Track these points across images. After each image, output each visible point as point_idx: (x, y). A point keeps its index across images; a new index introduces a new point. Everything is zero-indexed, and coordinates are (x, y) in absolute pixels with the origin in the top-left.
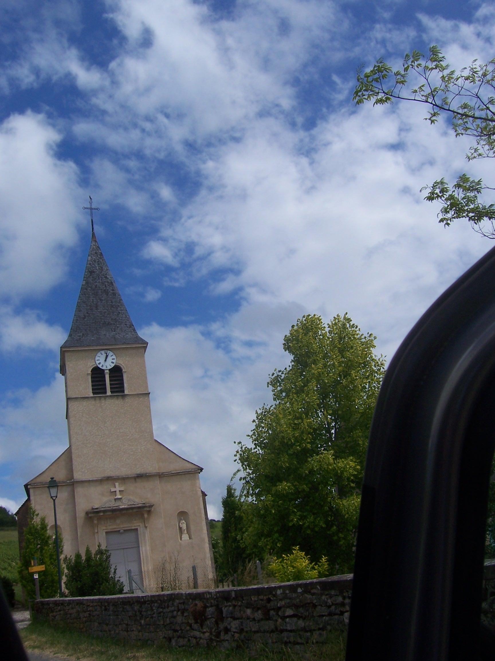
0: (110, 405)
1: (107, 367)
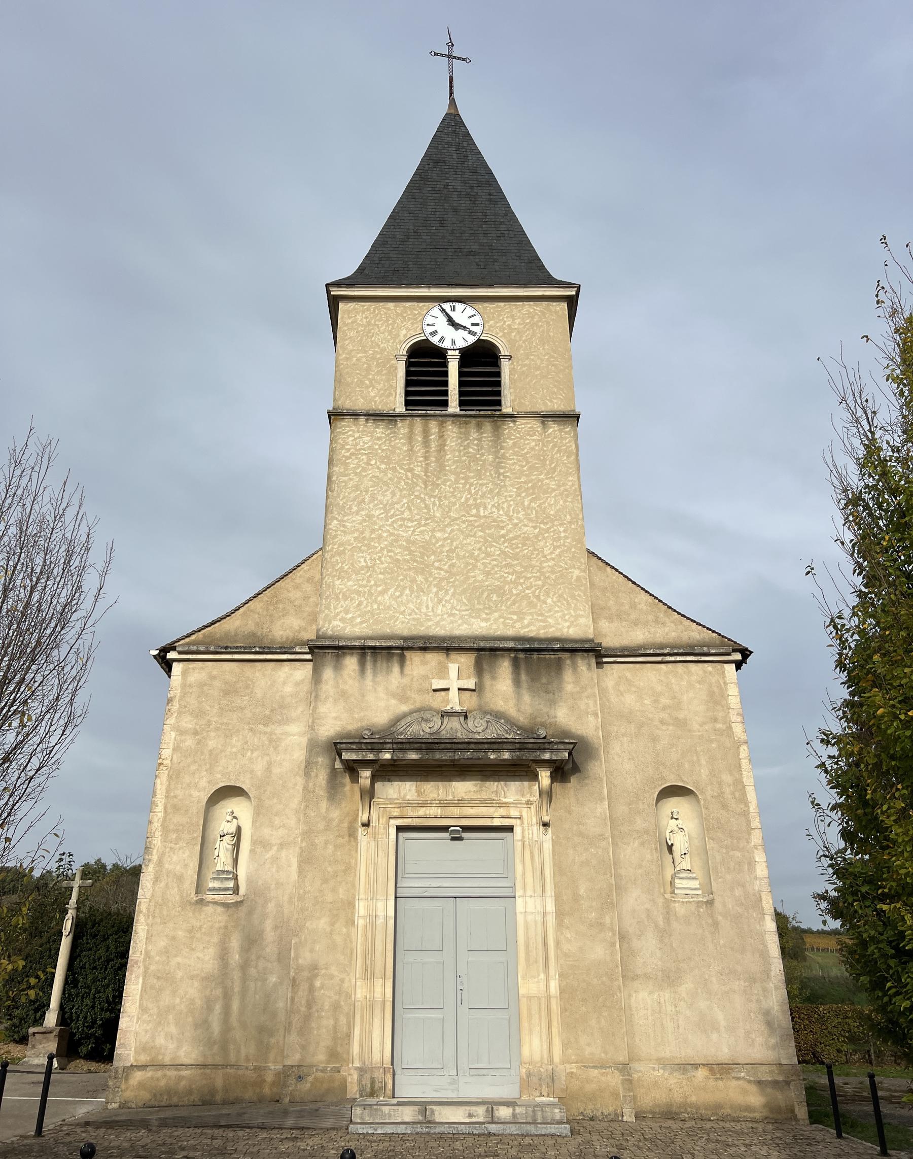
0: (454, 440)
1: (453, 342)
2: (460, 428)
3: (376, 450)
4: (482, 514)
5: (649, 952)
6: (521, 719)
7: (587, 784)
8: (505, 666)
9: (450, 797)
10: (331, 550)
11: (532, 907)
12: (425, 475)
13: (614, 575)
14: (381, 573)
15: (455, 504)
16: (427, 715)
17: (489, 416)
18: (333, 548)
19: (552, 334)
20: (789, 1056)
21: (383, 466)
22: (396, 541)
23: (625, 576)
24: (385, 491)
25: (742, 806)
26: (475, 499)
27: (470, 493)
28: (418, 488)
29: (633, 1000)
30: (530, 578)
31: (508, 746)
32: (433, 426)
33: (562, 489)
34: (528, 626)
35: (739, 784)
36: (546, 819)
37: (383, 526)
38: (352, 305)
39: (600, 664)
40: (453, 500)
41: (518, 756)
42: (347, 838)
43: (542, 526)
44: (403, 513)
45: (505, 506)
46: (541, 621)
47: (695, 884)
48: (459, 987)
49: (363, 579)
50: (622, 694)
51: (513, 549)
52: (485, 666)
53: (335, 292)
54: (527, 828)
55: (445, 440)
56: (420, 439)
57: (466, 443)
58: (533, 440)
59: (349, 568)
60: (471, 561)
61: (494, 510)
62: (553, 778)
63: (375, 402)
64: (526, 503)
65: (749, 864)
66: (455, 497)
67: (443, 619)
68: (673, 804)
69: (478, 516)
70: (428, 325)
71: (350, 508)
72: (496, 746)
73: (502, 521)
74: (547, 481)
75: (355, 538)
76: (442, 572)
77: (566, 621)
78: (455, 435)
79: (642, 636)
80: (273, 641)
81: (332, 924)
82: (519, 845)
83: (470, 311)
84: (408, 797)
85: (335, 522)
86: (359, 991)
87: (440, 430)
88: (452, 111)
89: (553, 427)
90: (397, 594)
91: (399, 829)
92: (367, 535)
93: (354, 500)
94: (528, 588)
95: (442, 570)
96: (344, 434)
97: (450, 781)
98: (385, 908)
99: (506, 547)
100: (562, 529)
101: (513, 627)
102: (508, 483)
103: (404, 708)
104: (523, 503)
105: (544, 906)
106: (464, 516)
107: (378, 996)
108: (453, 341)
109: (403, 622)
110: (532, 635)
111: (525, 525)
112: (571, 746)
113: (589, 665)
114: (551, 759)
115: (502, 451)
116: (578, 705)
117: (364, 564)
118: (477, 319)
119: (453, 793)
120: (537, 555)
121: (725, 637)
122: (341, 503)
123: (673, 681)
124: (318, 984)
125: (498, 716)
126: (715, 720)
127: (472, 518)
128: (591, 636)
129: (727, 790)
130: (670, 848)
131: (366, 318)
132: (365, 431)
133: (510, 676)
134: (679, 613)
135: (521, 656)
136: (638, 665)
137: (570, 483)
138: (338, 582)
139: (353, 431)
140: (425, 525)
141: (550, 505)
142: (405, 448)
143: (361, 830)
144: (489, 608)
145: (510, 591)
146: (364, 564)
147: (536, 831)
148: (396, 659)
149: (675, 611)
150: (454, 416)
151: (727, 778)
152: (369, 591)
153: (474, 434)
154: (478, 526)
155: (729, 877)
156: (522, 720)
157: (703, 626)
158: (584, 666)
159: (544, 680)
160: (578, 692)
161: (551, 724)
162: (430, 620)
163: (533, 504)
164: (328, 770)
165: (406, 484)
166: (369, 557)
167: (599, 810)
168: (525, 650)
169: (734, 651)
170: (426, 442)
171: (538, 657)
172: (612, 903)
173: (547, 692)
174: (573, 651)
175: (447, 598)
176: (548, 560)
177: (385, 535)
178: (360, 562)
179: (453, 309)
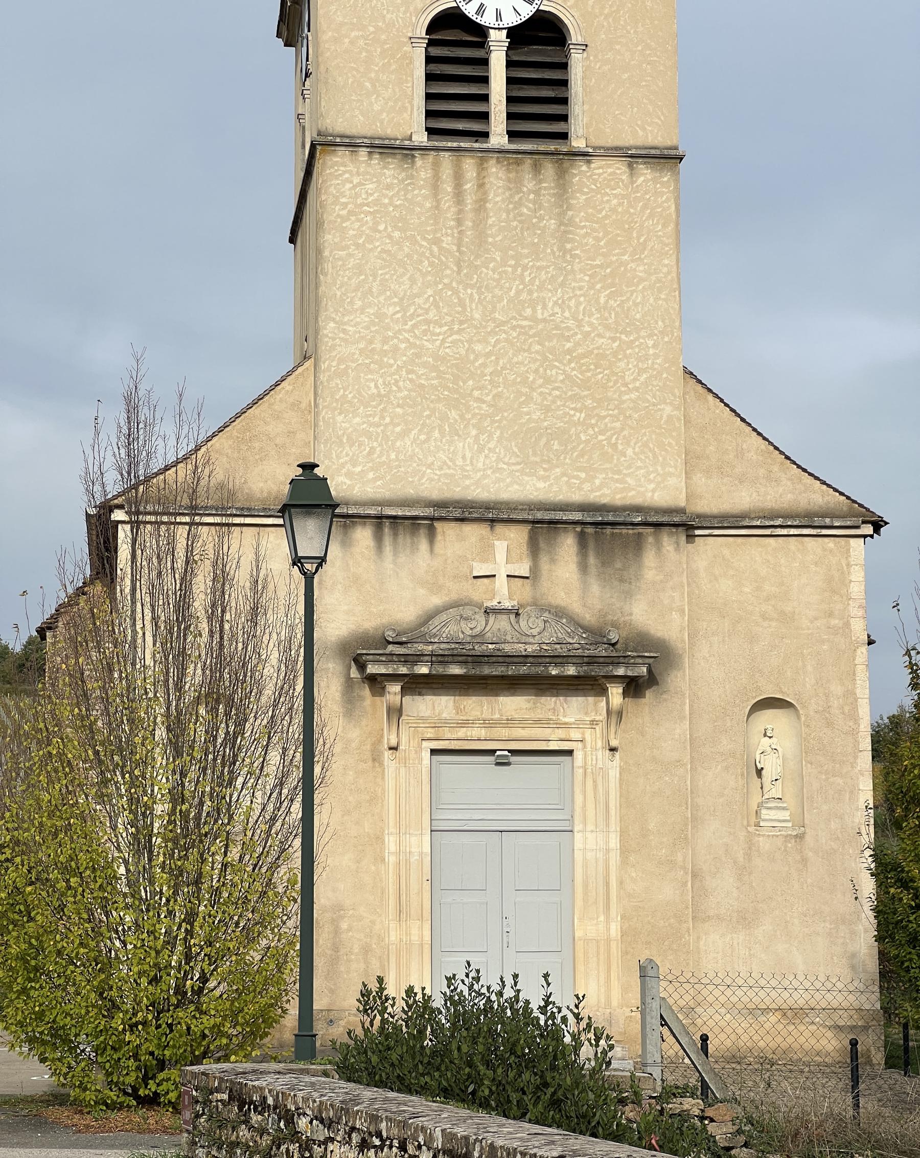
0: (498, 187)
1: (499, 16)
3: (386, 206)
4: (540, 316)
5: (724, 890)
6: (587, 616)
7: (665, 700)
8: (568, 544)
9: (497, 716)
10: (329, 369)
11: (594, 843)
12: (459, 250)
13: (717, 407)
14: (398, 406)
15: (501, 299)
16: (468, 612)
17: (552, 154)
18: (330, 366)
21: (397, 234)
22: (418, 356)
23: (732, 410)
24: (403, 275)
25: (851, 724)
26: (530, 292)
27: (523, 282)
28: (448, 272)
29: (702, 943)
30: (605, 417)
31: (574, 660)
32: (469, 165)
33: (653, 278)
34: (599, 488)
35: (851, 696)
36: (614, 743)
39: (691, 538)
40: (497, 292)
42: (370, 763)
43: (623, 337)
44: (427, 311)
45: (572, 303)
46: (617, 481)
47: (785, 815)
48: (505, 930)
49: (374, 416)
50: (716, 579)
51: (582, 373)
52: (542, 545)
54: (590, 751)
55: (485, 193)
56: (449, 189)
57: (517, 198)
58: (616, 196)
60: (524, 390)
61: (557, 309)
62: (625, 694)
63: (382, 122)
64: (602, 300)
65: (851, 792)
66: (502, 288)
67: (485, 476)
69: (533, 319)
71: (352, 303)
72: (559, 660)
73: (568, 329)
74: (633, 265)
75: (361, 351)
76: (484, 406)
78: (501, 183)
80: (250, 497)
82: (579, 772)
84: (444, 715)
85: (332, 325)
86: (392, 933)
87: (478, 174)
89: (645, 173)
90: (423, 437)
91: (434, 752)
92: (377, 345)
93: (356, 290)
94: (601, 433)
95: (484, 402)
96: (337, 178)
97: (497, 695)
98: (420, 843)
99: (573, 369)
100: (650, 343)
101: (580, 489)
102: (577, 267)
103: (436, 601)
104: (597, 301)
105: (607, 842)
106: (514, 318)
107: (415, 938)
109: (432, 480)
110: (605, 500)
111: (600, 336)
112: (651, 660)
113: (678, 544)
115: (570, 213)
116: (661, 595)
117: (375, 391)
119: (500, 710)
120: (616, 382)
121: (854, 502)
122: (339, 293)
123: (782, 561)
124: (344, 926)
125: (559, 613)
126: (831, 615)
127: (525, 323)
128: (682, 503)
129: (835, 704)
130: (759, 772)
133: (575, 559)
134: (799, 467)
135: (590, 530)
136: (740, 539)
137: (665, 270)
138: (340, 418)
139: (350, 172)
140: (459, 332)
141: (636, 305)
142: (428, 205)
143: (387, 754)
144: (549, 462)
145: (577, 435)
146: (375, 391)
148: (423, 532)
149: (794, 463)
150: (500, 151)
151: (837, 689)
152: (383, 431)
153: (529, 184)
154: (534, 336)
155: (825, 807)
156: (589, 618)
157: (829, 486)
158: (669, 542)
159: (618, 565)
160: (661, 581)
161: (625, 623)
162: (468, 477)
163: (611, 302)
164: (342, 680)
165: (431, 264)
166: (381, 381)
167: (678, 731)
168: (595, 524)
169: (863, 522)
170: (459, 194)
171: (611, 532)
172: (686, 838)
173: (622, 580)
174: (658, 525)
176: (630, 391)
177: (403, 346)
178: (369, 388)
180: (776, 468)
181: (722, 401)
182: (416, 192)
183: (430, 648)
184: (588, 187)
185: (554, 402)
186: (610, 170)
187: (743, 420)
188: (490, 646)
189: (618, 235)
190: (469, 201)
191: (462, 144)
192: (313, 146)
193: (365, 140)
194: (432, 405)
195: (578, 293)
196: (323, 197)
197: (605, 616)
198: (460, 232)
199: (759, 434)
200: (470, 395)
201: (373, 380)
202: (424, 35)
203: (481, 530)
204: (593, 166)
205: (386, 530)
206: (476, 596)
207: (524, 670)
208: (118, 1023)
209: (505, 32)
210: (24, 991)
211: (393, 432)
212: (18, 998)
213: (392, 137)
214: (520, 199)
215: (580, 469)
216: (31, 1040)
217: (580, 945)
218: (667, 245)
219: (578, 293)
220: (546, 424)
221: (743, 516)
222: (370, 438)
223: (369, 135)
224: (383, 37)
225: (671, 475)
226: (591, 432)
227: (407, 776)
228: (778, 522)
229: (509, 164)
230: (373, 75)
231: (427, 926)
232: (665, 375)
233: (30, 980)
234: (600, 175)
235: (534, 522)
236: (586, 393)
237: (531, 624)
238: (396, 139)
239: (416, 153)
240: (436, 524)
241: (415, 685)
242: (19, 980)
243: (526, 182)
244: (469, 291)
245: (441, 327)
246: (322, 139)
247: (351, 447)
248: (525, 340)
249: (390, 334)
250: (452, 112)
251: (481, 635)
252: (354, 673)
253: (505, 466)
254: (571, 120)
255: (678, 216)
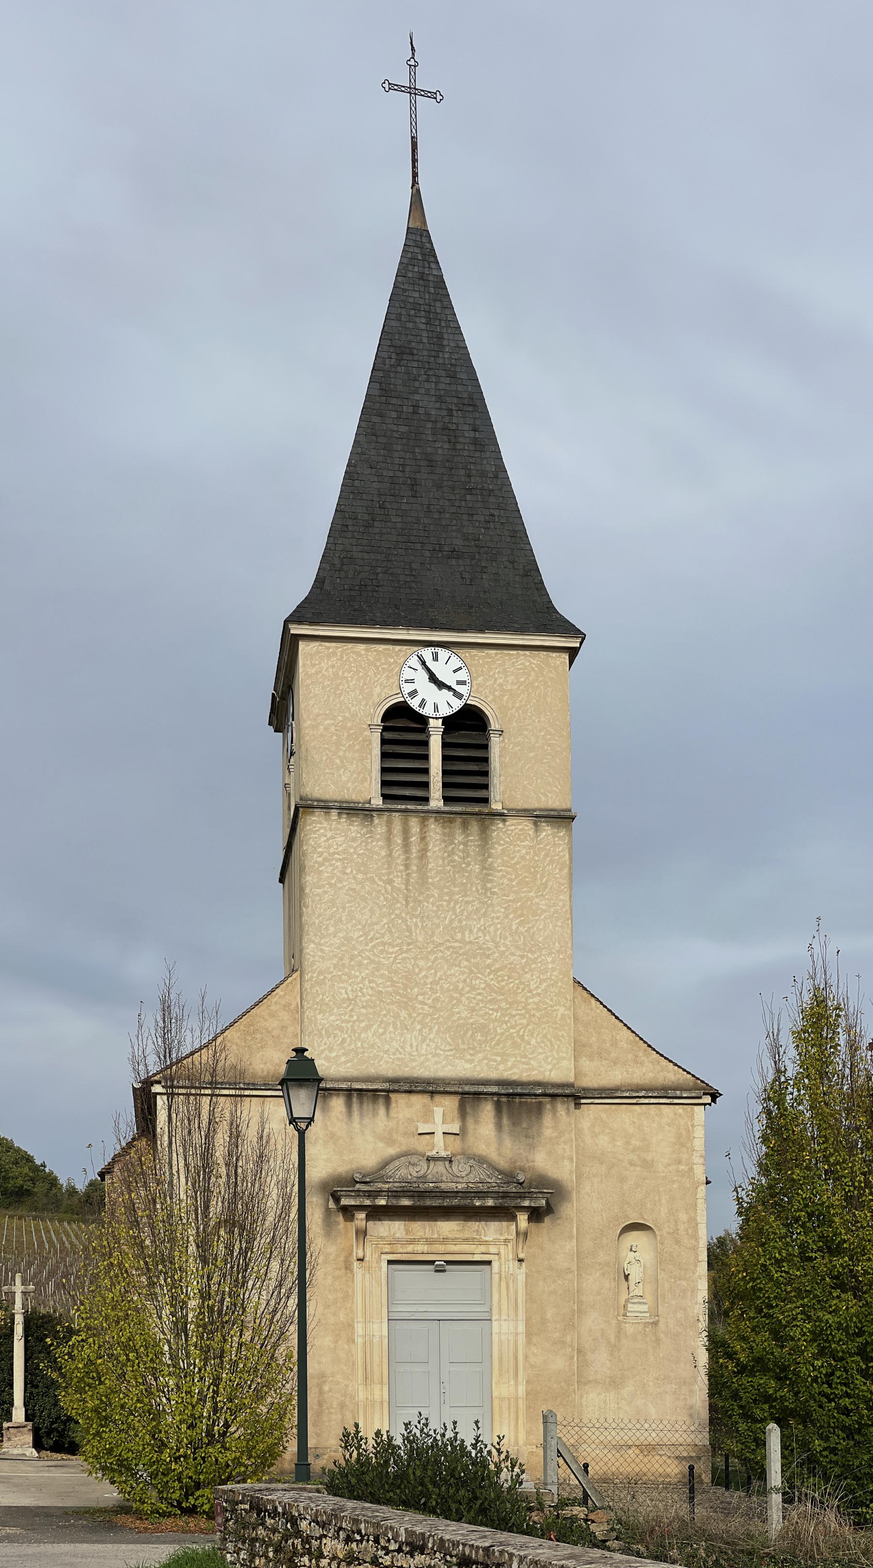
1: (436, 708)
2: (444, 827)
3: (351, 855)
4: (467, 940)
5: (601, 1362)
7: (559, 1224)
8: (488, 1110)
9: (436, 1236)
10: (311, 979)
11: (507, 1329)
12: (406, 889)
13: (598, 1008)
14: (363, 1007)
15: (438, 926)
16: (414, 1159)
17: (477, 814)
18: (312, 977)
19: (549, 700)
20: (703, 1438)
21: (360, 876)
22: (378, 970)
24: (364, 908)
25: (693, 1242)
26: (460, 921)
27: (455, 913)
28: (399, 905)
29: (584, 1399)
31: (493, 1195)
32: (414, 823)
33: (552, 910)
34: (511, 1068)
35: (693, 1221)
36: (521, 1256)
37: (363, 951)
38: (314, 645)
39: (578, 1105)
41: (501, 1203)
42: (343, 1271)
43: (529, 955)
44: (383, 935)
46: (524, 1063)
47: (644, 1308)
48: (442, 1391)
50: (596, 1136)
51: (498, 982)
52: (468, 1110)
53: (295, 630)
55: (426, 844)
56: (399, 841)
57: (450, 848)
58: (524, 847)
59: (330, 1001)
60: (456, 995)
61: (480, 934)
62: (530, 1220)
63: (348, 790)
64: (514, 927)
65: (692, 1291)
66: (439, 917)
67: (427, 1060)
68: (633, 1238)
70: (407, 681)
71: (327, 929)
72: (482, 1195)
73: (489, 949)
74: (537, 900)
75: (335, 966)
76: (426, 1007)
77: (549, 1063)
78: (438, 837)
79: (620, 1077)
81: (336, 1342)
82: (496, 1277)
83: (455, 662)
84: (397, 1235)
85: (312, 945)
87: (421, 830)
88: (418, 224)
89: (547, 830)
90: (381, 1031)
91: (390, 1262)
92: (346, 961)
93: (329, 919)
94: (513, 1027)
95: (426, 1004)
96: (315, 832)
98: (380, 1329)
99: (492, 980)
100: (549, 959)
101: (497, 1069)
103: (391, 1151)
105: (516, 1328)
106: (448, 941)
107: (377, 1397)
108: (437, 705)
109: (387, 1062)
110: (515, 1078)
111: (513, 954)
112: (549, 1195)
113: (568, 1109)
114: (526, 1201)
115: (490, 860)
116: (556, 1148)
117: (345, 996)
118: (463, 675)
119: (438, 1232)
120: (523, 990)
121: (698, 1079)
122: (317, 921)
123: (645, 1123)
124: (326, 1388)
125: (481, 1160)
126: (680, 1162)
128: (572, 1080)
129: (682, 1227)
130: (627, 1277)
131: (333, 666)
132: (338, 829)
133: (493, 1120)
134: (658, 1053)
135: (504, 1099)
136: (614, 1107)
137: (561, 904)
138: (320, 1017)
139: (325, 828)
140: (408, 951)
141: (539, 930)
142: (383, 853)
143: (356, 1264)
144: (474, 1048)
145: (495, 1029)
146: (345, 996)
147: (513, 1265)
148: (381, 1101)
149: (654, 1050)
150: (438, 812)
151: (683, 1217)
152: (352, 1026)
153: (459, 838)
155: (673, 1302)
156: (503, 1164)
157: (679, 1067)
158: (561, 1108)
159: (525, 1125)
162: (414, 1060)
163: (521, 929)
164: (323, 1210)
165: (386, 899)
166: (350, 988)
167: (568, 1247)
168: (508, 1095)
169: (704, 1094)
170: (406, 845)
171: (520, 1101)
172: (573, 1325)
173: (527, 1137)
174: (554, 1096)
175: (432, 1036)
176: (533, 996)
178: (341, 994)
179: (436, 658)
180: (641, 1054)
181: (601, 1003)
182: (374, 843)
183: (387, 1186)
184: (503, 839)
185: (477, 1004)
186: (520, 827)
187: (617, 1018)
188: (431, 1185)
189: (526, 877)
190: (414, 850)
191: (409, 807)
192: (297, 809)
193: (336, 804)
194: (387, 1007)
195: (497, 921)
196: (305, 848)
197: (515, 1162)
198: (408, 875)
199: (629, 1028)
200: (416, 999)
201: (344, 988)
202: (379, 723)
203: (424, 1099)
204: (507, 823)
205: (355, 1100)
206: (420, 1149)
207: (455, 1202)
208: (166, 1456)
209: (440, 721)
210: (98, 1433)
211: (359, 1026)
212: (93, 1438)
213: (356, 800)
214: (453, 849)
215: (497, 1054)
216: (104, 1469)
217: (496, 1403)
218: (562, 885)
219: (497, 921)
220: (471, 1021)
221: (617, 1089)
222: (342, 1031)
223: (339, 799)
224: (349, 724)
225: (564, 1058)
226: (505, 1026)
227: (370, 1282)
228: (642, 1094)
229: (444, 822)
230: (341, 753)
231: (386, 1389)
232: (560, 984)
233: (102, 1426)
234: (512, 830)
235: (463, 1093)
236: (501, 997)
237: (460, 1169)
238: (359, 803)
239: (374, 814)
240: (391, 1095)
241: (376, 1213)
242: (94, 1426)
243: (457, 836)
244: (414, 920)
245: (393, 947)
246: (303, 803)
247: (328, 1037)
248: (457, 958)
249: (356, 953)
250: (401, 781)
251: (424, 1176)
252: (332, 1205)
253: (441, 1052)
254: (492, 788)
255: (571, 862)
